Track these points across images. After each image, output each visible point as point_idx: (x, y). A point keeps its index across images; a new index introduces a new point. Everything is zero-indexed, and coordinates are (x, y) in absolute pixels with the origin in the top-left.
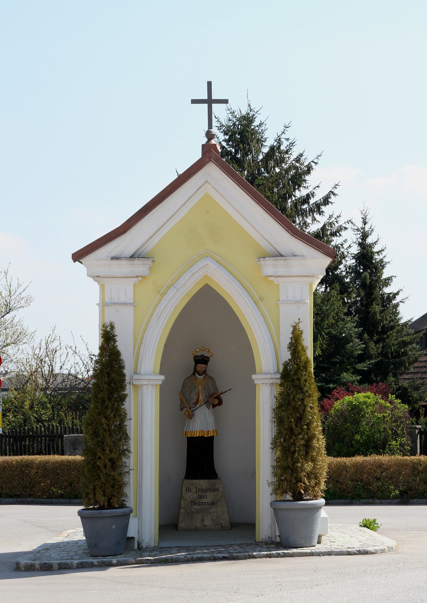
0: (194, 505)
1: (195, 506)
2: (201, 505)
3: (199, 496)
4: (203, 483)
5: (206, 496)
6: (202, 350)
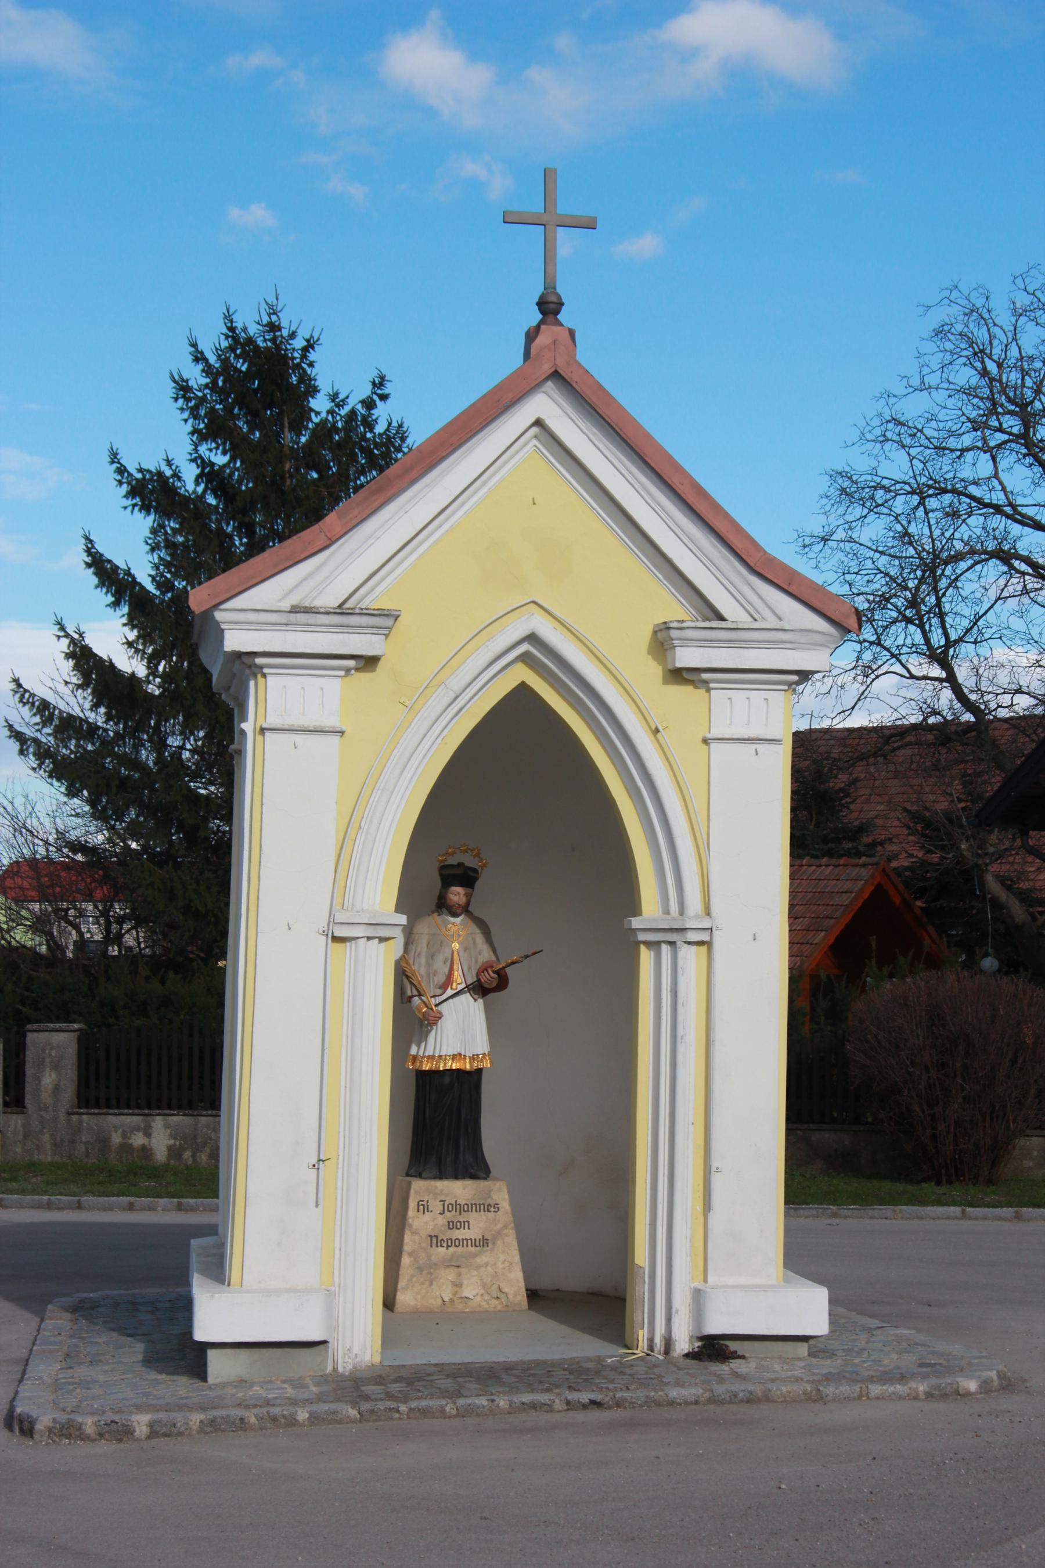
0: (437, 1246)
1: (440, 1249)
2: (456, 1246)
3: (449, 1222)
4: (460, 1190)
5: (466, 1224)
6: (462, 851)
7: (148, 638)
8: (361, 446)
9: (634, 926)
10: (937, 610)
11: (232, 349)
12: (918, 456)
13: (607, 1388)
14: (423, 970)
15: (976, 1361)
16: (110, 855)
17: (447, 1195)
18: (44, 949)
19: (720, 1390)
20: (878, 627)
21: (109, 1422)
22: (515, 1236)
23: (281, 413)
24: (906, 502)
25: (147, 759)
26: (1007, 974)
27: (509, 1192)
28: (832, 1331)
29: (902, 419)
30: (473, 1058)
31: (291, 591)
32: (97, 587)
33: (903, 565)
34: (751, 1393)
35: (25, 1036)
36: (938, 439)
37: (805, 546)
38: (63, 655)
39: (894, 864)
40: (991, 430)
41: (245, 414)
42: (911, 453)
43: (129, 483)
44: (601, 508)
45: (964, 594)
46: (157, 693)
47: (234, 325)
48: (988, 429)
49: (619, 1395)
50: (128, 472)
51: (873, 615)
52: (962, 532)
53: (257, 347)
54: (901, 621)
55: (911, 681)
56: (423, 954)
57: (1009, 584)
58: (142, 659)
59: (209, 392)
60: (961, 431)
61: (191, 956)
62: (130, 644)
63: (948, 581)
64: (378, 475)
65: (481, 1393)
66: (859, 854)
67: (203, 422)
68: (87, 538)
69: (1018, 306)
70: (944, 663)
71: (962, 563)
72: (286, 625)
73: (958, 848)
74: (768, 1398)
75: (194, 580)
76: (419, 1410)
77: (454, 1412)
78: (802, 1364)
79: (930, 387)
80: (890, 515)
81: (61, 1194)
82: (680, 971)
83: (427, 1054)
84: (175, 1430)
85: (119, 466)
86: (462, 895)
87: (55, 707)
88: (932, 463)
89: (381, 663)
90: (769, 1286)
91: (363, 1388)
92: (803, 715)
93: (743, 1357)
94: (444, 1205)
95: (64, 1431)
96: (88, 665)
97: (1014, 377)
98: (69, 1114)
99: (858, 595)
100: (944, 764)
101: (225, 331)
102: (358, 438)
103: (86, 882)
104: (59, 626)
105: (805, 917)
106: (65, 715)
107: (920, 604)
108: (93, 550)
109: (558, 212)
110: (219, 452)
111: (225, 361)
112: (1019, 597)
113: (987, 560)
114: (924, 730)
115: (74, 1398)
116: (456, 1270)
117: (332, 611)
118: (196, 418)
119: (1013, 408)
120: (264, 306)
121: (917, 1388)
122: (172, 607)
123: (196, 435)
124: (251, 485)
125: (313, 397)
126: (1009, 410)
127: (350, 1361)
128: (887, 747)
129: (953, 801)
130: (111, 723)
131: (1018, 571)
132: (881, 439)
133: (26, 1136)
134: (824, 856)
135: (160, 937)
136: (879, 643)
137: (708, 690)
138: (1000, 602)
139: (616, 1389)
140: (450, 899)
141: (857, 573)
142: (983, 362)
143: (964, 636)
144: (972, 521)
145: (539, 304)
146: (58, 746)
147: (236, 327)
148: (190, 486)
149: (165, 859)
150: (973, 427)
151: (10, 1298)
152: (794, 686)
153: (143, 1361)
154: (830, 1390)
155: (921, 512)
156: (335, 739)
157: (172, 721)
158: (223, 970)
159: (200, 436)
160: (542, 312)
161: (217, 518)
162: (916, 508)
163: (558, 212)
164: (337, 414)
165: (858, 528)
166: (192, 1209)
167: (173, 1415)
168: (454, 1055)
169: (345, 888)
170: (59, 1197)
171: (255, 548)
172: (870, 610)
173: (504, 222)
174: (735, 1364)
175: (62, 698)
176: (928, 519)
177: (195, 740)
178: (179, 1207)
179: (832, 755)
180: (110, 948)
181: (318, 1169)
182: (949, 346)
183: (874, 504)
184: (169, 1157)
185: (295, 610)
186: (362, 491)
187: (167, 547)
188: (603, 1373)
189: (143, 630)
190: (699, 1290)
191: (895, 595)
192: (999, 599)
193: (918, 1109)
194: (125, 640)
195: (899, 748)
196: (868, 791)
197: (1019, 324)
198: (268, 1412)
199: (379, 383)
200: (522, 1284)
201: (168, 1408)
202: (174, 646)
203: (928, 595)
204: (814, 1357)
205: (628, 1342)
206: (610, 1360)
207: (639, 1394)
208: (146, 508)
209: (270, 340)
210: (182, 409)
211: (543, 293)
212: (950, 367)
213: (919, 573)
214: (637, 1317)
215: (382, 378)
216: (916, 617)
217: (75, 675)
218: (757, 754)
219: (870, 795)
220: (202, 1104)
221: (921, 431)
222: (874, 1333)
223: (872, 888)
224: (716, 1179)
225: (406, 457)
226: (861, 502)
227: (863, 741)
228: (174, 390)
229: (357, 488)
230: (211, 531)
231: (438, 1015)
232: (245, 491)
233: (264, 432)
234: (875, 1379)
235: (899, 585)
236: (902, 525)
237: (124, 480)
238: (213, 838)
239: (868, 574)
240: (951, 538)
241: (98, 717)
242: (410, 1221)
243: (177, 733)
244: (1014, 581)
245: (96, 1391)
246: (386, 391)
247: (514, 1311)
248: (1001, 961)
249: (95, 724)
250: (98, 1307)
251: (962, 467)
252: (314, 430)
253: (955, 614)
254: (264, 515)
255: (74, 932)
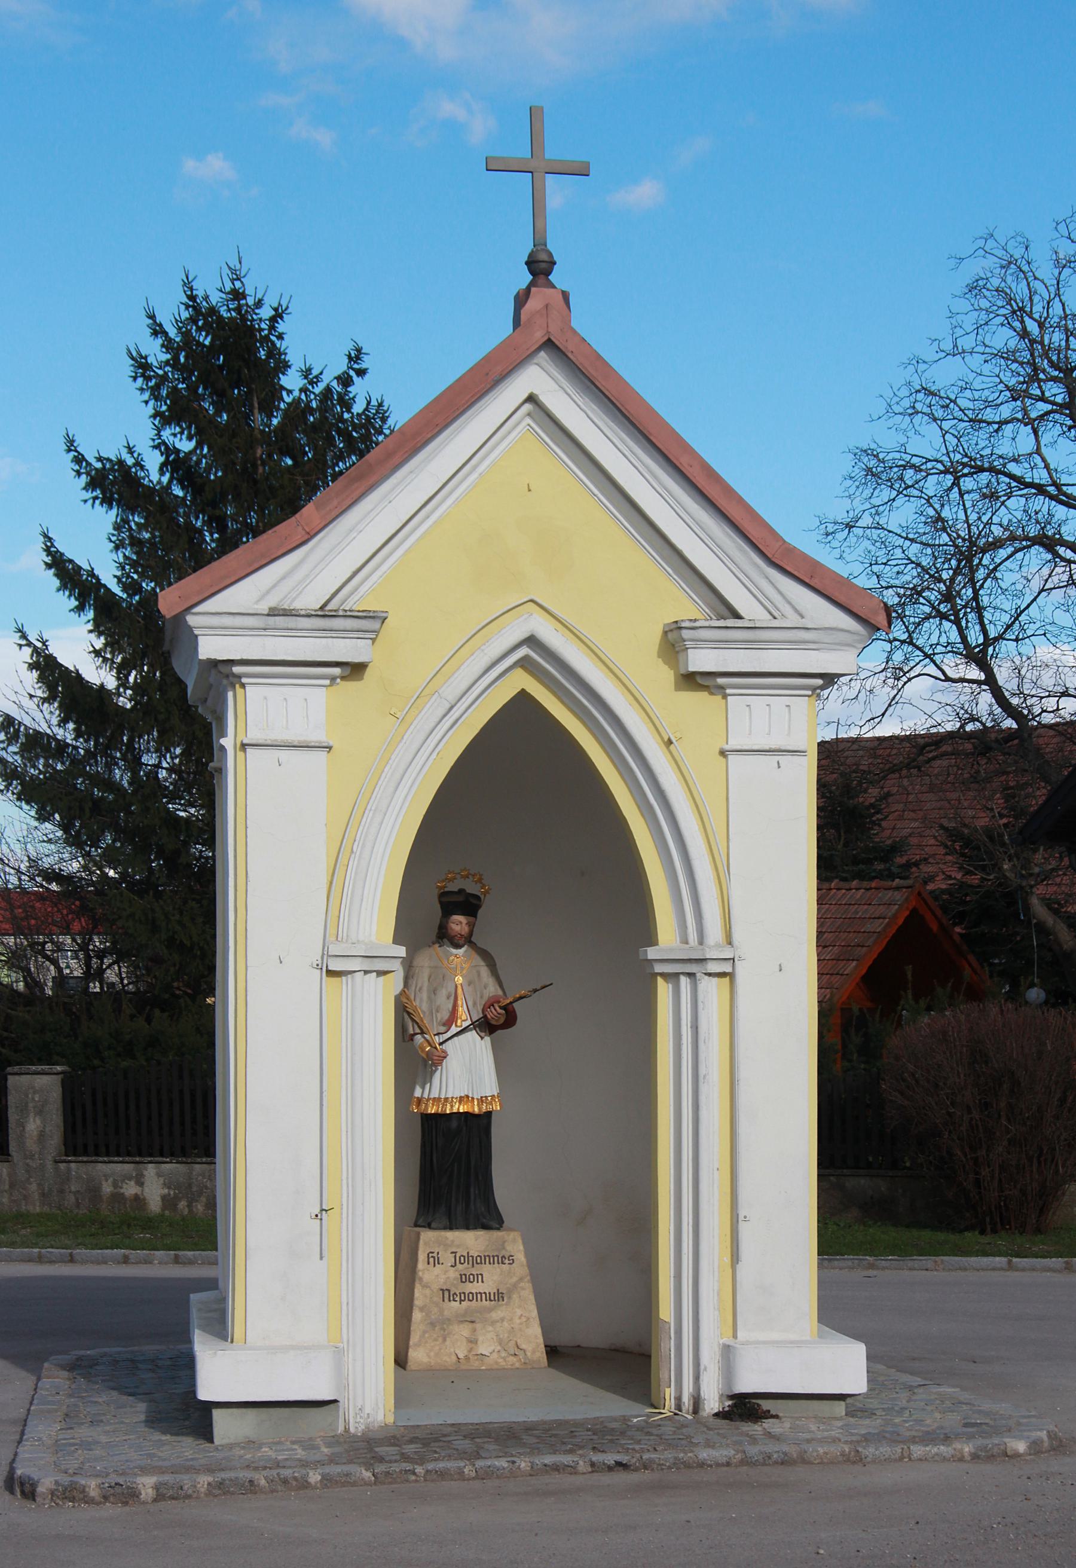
0: (450, 1301)
1: (453, 1303)
2: (469, 1300)
3: (461, 1275)
4: (472, 1240)
5: (480, 1277)
6: (462, 877)
7: (116, 646)
8: (339, 428)
9: (649, 957)
10: (974, 604)
11: (193, 320)
12: (950, 431)
13: (633, 1449)
14: (425, 1006)
15: (1025, 1420)
16: (86, 884)
17: (458, 1246)
18: (21, 986)
19: (753, 1451)
20: (909, 624)
21: (113, 1484)
22: (531, 1289)
23: (249, 393)
24: (939, 483)
25: (121, 779)
26: (1054, 1006)
27: (524, 1244)
28: (870, 1389)
29: (933, 389)
30: (481, 1100)
31: (268, 592)
32: (59, 590)
33: (936, 554)
34: (785, 1454)
35: (6, 1080)
36: (974, 410)
37: (827, 534)
38: (27, 665)
39: (930, 887)
40: (1032, 399)
41: (210, 393)
42: (943, 427)
43: (88, 474)
44: (603, 494)
45: (1004, 585)
46: (129, 706)
47: (195, 292)
48: (1029, 398)
49: (646, 1456)
50: (87, 461)
51: (904, 611)
52: (1001, 516)
53: (221, 317)
54: (934, 617)
55: (946, 684)
56: (425, 988)
57: (1053, 574)
58: (111, 669)
59: (170, 369)
60: (999, 401)
61: (177, 992)
62: (97, 653)
63: (986, 571)
64: (358, 460)
65: (501, 1454)
66: (892, 876)
67: (166, 404)
68: (46, 536)
69: (1061, 256)
70: (983, 664)
71: (1001, 551)
72: (265, 629)
73: (1000, 869)
74: (803, 1460)
75: (163, 579)
76: (437, 1472)
77: (473, 1474)
78: (840, 1424)
79: (964, 352)
80: (921, 497)
81: (52, 1247)
82: (700, 1005)
83: (432, 1096)
84: (182, 1493)
85: (76, 454)
86: (464, 925)
87: (20, 723)
88: (967, 438)
89: (368, 670)
90: (802, 1342)
91: (377, 1449)
92: (829, 723)
93: (776, 1417)
94: (455, 1257)
95: (67, 1494)
96: (54, 676)
97: (1057, 338)
98: (56, 1162)
99: (887, 588)
100: (984, 775)
101: (185, 300)
102: (335, 419)
103: (62, 914)
104: (20, 634)
105: (835, 946)
106: (31, 731)
107: (955, 597)
108: (53, 549)
109: (547, 156)
110: (184, 437)
111: (186, 335)
112: (1064, 589)
113: (1029, 547)
114: (961, 739)
115: (76, 1459)
116: (471, 1325)
117: (313, 613)
118: (157, 398)
119: (1056, 373)
120: (226, 270)
121: (962, 1449)
122: (140, 611)
123: (158, 418)
124: (220, 474)
125: (284, 374)
126: (1052, 376)
127: (362, 1421)
128: (921, 758)
129: (994, 817)
130: (81, 740)
131: (1063, 559)
132: (910, 411)
133: (12, 1185)
134: (854, 879)
135: (144, 972)
136: (911, 643)
137: (725, 696)
138: (1044, 594)
139: (642, 1451)
140: (451, 928)
141: (885, 564)
142: (1022, 322)
143: (1004, 633)
144: (1012, 503)
145: (527, 263)
146: (25, 765)
147: (197, 295)
148: (155, 476)
149: (145, 888)
150: (1012, 396)
151: (6, 1357)
152: (818, 691)
153: (146, 1421)
154: (869, 1451)
155: (955, 494)
156: (322, 755)
157: (146, 737)
158: (212, 1008)
159: (164, 419)
160: (532, 272)
161: (185, 512)
162: (950, 489)
163: (547, 156)
164: (311, 392)
165: (886, 512)
166: (191, 1262)
167: (179, 1477)
168: (461, 1097)
169: (339, 917)
170: (49, 1250)
171: (228, 544)
172: (901, 605)
173: (487, 170)
174: (768, 1424)
175: (27, 713)
176: (963, 502)
177: (172, 758)
178: (177, 1260)
179: (861, 767)
180: (91, 985)
181: (321, 1219)
182: (984, 304)
183: (903, 485)
184: (164, 1207)
185: (273, 613)
186: (341, 478)
187: (132, 544)
188: (629, 1433)
189: (111, 637)
190: (729, 1346)
191: (928, 588)
192: (1043, 590)
193: (959, 1153)
194: (91, 649)
195: (934, 758)
196: (901, 806)
197: (1062, 278)
198: (278, 1474)
199: (356, 356)
200: (541, 1340)
201: (174, 1470)
202: (144, 655)
203: (964, 587)
204: (852, 1417)
205: (654, 1400)
206: (635, 1420)
207: (667, 1456)
208: (108, 501)
209: (234, 310)
210: (142, 390)
211: (532, 251)
212: (986, 328)
213: (954, 563)
214: (663, 1375)
215: (359, 350)
216: (951, 612)
217: (40, 688)
218: (779, 767)
219: (904, 811)
220: (196, 1151)
221: (954, 402)
222: (916, 1391)
223: (908, 913)
224: (743, 1227)
225: (389, 439)
226: (889, 484)
227: (894, 752)
228: (132, 368)
229: (336, 476)
230: (179, 526)
231: (443, 1055)
232: (214, 481)
233: (232, 414)
234: (917, 1439)
235: (931, 576)
236: (934, 509)
237: (82, 471)
238: (195, 865)
239: (897, 565)
240: (989, 523)
241: (67, 734)
242: (420, 1274)
243: (152, 750)
244: (1058, 570)
245: (98, 1452)
246: (364, 366)
247: (533, 1368)
248: (1048, 992)
249: (64, 741)
250: (97, 1364)
251: (1000, 442)
252: (286, 411)
253: (994, 608)
254: (235, 507)
255: (52, 968)
